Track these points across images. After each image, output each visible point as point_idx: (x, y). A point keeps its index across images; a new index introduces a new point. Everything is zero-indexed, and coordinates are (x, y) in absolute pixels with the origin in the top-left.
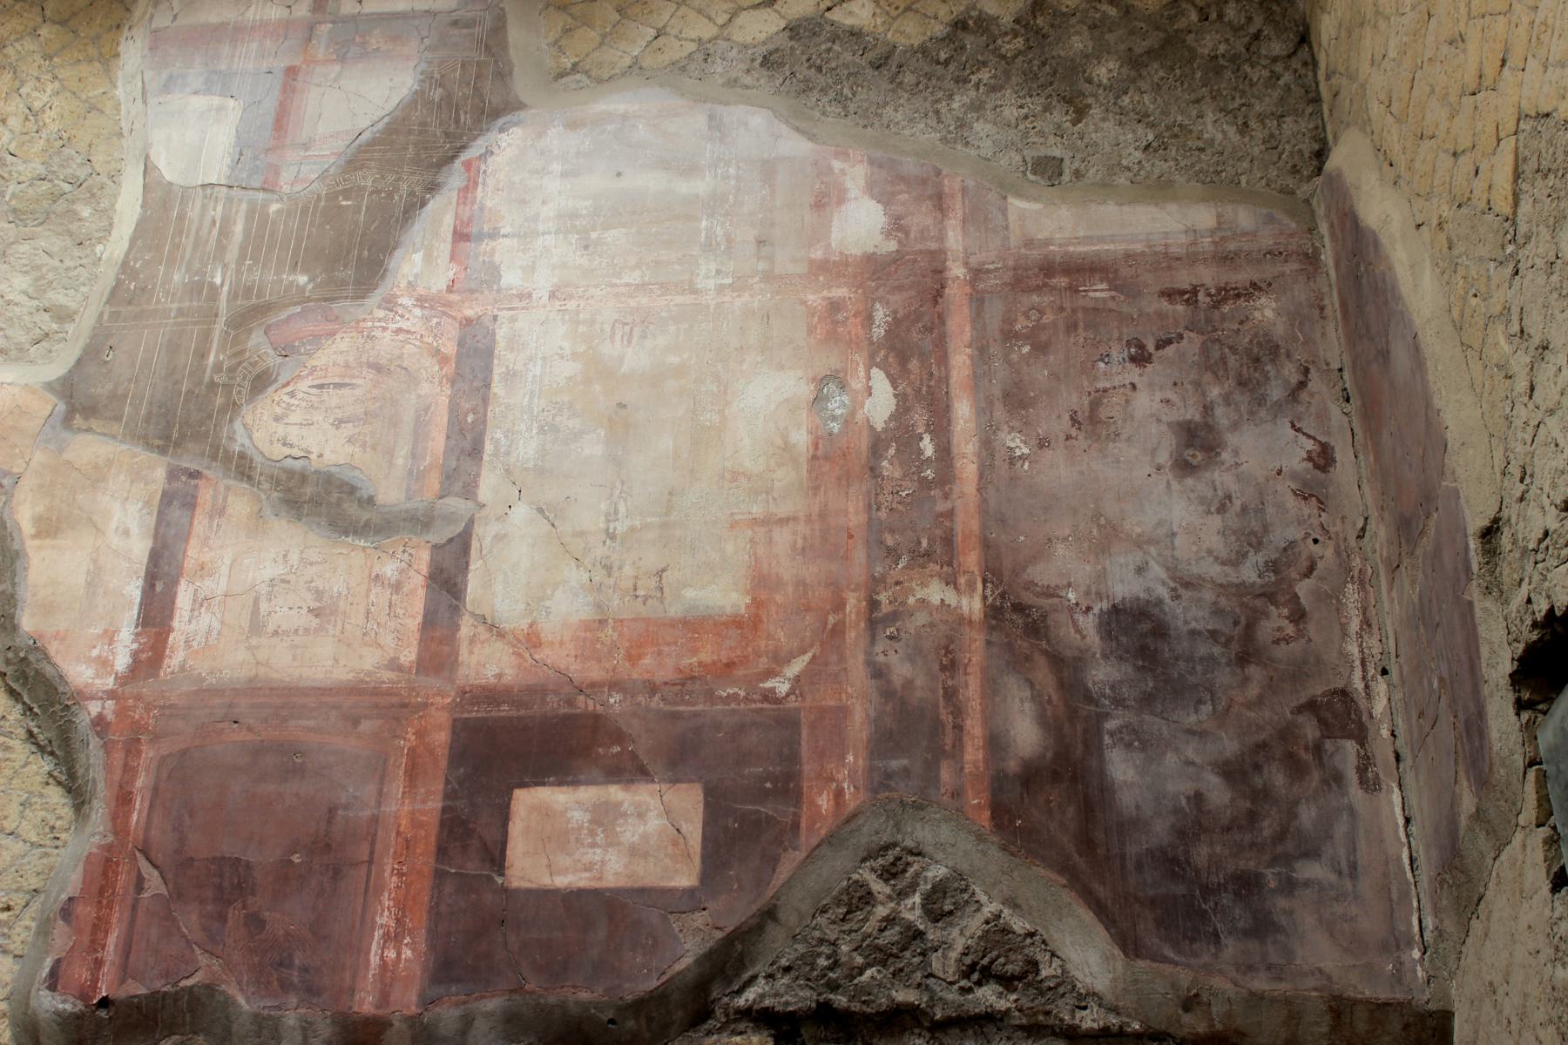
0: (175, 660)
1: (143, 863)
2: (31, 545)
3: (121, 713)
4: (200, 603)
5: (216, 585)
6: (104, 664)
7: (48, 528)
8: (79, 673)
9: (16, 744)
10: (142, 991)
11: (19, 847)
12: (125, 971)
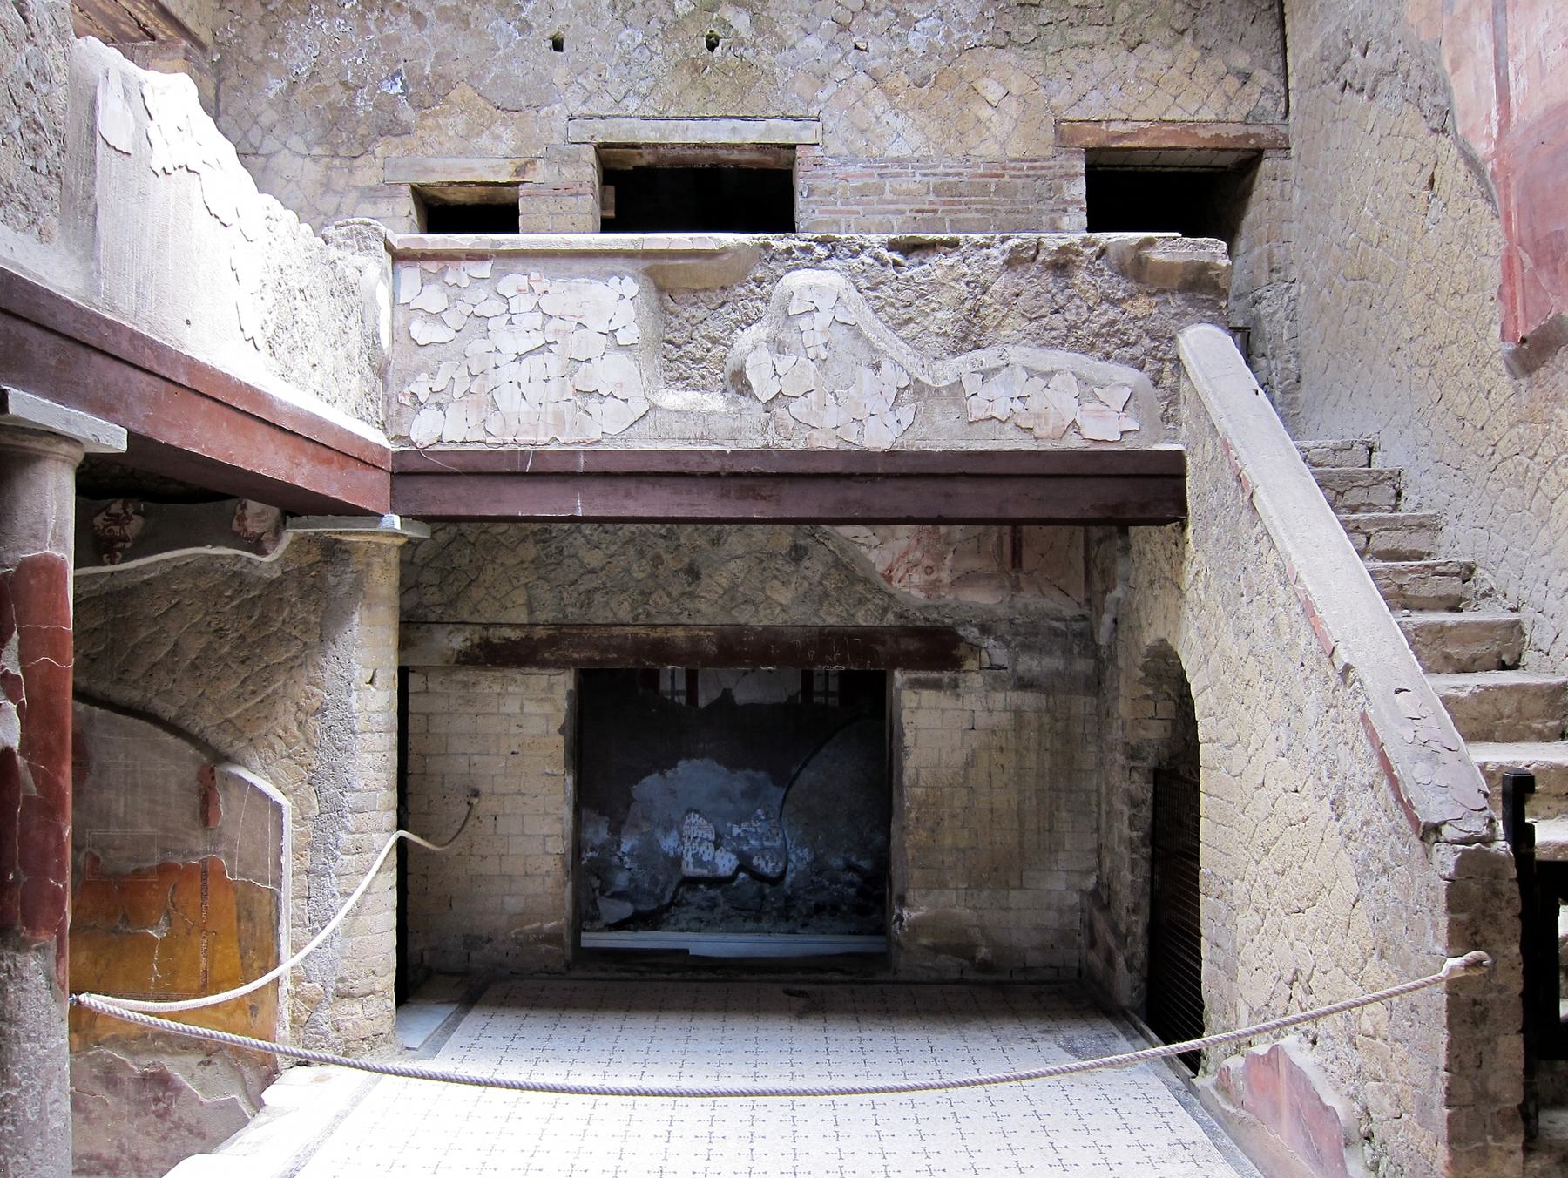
0: (1513, 119)
1: (1522, 253)
2: (1452, 79)
3: (1500, 164)
4: (1517, 73)
5: (1521, 57)
6: (1489, 136)
7: (1456, 65)
8: (1482, 148)
9: (1479, 201)
10: (1534, 328)
11: (1489, 261)
12: (1528, 320)
